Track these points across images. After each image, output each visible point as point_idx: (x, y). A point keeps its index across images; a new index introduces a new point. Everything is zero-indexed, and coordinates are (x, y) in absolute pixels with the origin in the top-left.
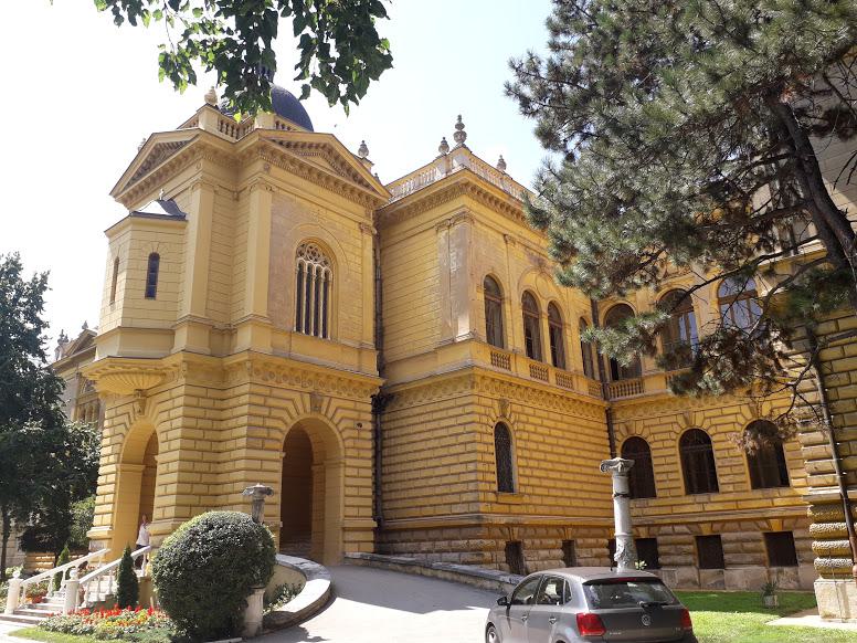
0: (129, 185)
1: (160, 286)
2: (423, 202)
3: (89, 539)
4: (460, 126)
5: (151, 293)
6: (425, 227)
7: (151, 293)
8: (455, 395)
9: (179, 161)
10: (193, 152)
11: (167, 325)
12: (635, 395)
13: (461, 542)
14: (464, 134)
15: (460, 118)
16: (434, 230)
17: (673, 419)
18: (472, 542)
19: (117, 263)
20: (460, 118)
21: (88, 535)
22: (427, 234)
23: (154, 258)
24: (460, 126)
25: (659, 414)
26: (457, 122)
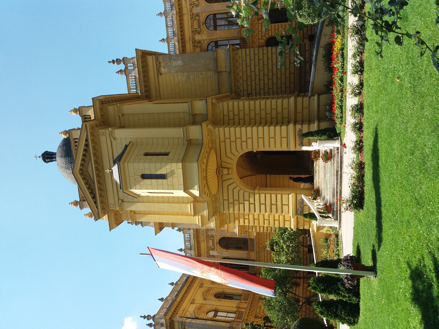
0: (95, 202)
1: (163, 151)
2: (145, 87)
3: (297, 229)
4: (113, 62)
5: (167, 154)
6: (157, 82)
7: (167, 154)
8: (240, 61)
9: (94, 148)
10: (92, 135)
11: (186, 143)
12: (248, 44)
13: (307, 56)
14: (117, 59)
15: (109, 62)
16: (160, 77)
17: (260, 25)
18: (307, 49)
19: (144, 177)
20: (109, 62)
21: (295, 230)
22: (160, 79)
23: (146, 154)
24: (113, 62)
25: (257, 32)
26: (111, 63)
